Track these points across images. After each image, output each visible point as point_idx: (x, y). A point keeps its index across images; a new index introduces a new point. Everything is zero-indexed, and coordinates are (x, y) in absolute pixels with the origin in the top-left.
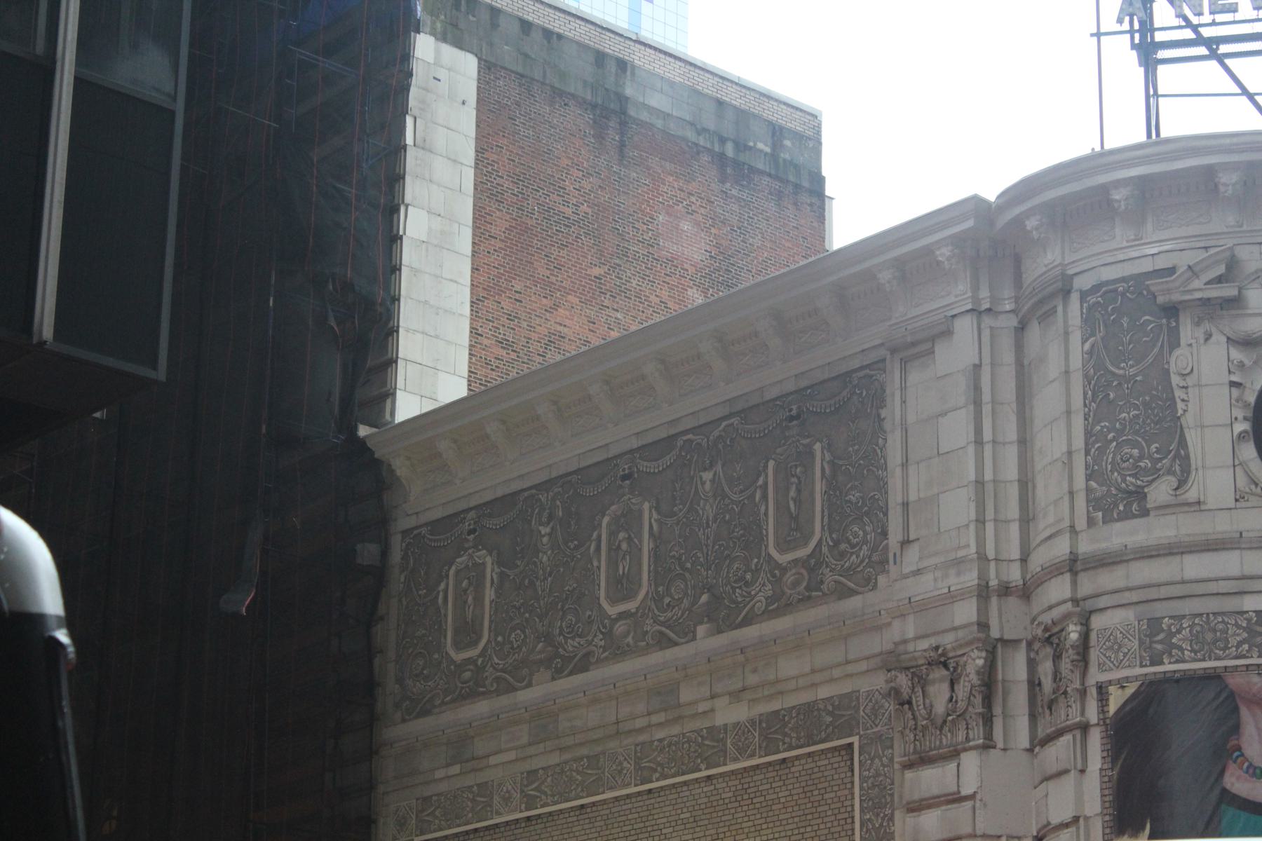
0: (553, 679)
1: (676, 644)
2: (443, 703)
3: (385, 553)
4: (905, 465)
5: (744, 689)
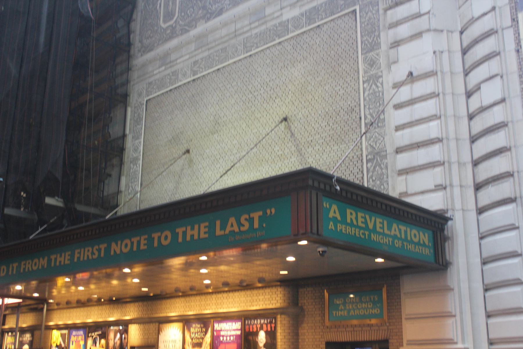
0: (206, 22)
2: (158, 44)
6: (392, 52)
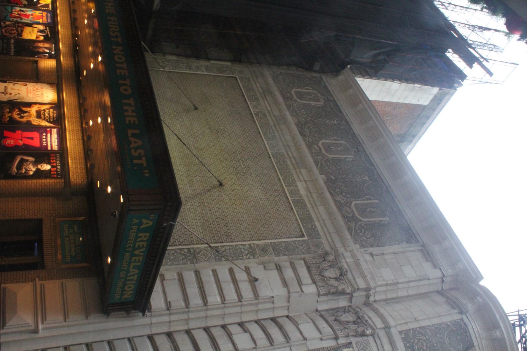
0: (295, 124)
1: (317, 167)
3: (315, 71)
4: (394, 253)
5: (310, 193)
6: (273, 265)
